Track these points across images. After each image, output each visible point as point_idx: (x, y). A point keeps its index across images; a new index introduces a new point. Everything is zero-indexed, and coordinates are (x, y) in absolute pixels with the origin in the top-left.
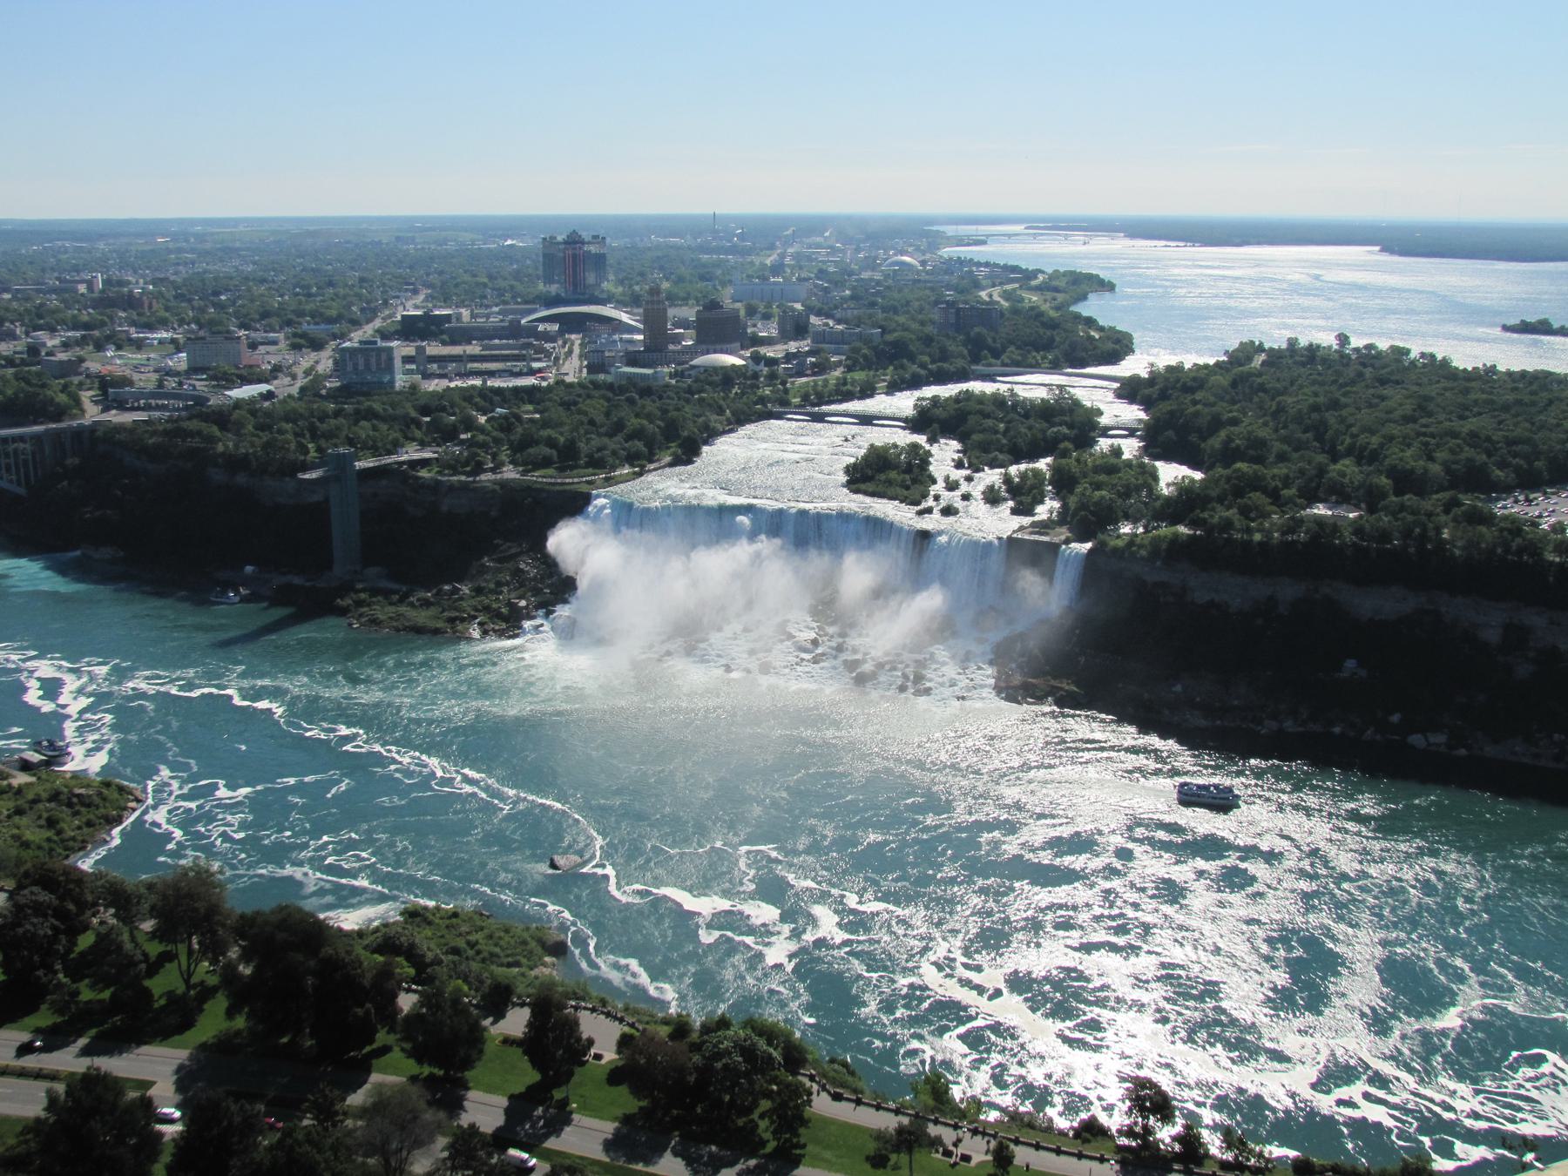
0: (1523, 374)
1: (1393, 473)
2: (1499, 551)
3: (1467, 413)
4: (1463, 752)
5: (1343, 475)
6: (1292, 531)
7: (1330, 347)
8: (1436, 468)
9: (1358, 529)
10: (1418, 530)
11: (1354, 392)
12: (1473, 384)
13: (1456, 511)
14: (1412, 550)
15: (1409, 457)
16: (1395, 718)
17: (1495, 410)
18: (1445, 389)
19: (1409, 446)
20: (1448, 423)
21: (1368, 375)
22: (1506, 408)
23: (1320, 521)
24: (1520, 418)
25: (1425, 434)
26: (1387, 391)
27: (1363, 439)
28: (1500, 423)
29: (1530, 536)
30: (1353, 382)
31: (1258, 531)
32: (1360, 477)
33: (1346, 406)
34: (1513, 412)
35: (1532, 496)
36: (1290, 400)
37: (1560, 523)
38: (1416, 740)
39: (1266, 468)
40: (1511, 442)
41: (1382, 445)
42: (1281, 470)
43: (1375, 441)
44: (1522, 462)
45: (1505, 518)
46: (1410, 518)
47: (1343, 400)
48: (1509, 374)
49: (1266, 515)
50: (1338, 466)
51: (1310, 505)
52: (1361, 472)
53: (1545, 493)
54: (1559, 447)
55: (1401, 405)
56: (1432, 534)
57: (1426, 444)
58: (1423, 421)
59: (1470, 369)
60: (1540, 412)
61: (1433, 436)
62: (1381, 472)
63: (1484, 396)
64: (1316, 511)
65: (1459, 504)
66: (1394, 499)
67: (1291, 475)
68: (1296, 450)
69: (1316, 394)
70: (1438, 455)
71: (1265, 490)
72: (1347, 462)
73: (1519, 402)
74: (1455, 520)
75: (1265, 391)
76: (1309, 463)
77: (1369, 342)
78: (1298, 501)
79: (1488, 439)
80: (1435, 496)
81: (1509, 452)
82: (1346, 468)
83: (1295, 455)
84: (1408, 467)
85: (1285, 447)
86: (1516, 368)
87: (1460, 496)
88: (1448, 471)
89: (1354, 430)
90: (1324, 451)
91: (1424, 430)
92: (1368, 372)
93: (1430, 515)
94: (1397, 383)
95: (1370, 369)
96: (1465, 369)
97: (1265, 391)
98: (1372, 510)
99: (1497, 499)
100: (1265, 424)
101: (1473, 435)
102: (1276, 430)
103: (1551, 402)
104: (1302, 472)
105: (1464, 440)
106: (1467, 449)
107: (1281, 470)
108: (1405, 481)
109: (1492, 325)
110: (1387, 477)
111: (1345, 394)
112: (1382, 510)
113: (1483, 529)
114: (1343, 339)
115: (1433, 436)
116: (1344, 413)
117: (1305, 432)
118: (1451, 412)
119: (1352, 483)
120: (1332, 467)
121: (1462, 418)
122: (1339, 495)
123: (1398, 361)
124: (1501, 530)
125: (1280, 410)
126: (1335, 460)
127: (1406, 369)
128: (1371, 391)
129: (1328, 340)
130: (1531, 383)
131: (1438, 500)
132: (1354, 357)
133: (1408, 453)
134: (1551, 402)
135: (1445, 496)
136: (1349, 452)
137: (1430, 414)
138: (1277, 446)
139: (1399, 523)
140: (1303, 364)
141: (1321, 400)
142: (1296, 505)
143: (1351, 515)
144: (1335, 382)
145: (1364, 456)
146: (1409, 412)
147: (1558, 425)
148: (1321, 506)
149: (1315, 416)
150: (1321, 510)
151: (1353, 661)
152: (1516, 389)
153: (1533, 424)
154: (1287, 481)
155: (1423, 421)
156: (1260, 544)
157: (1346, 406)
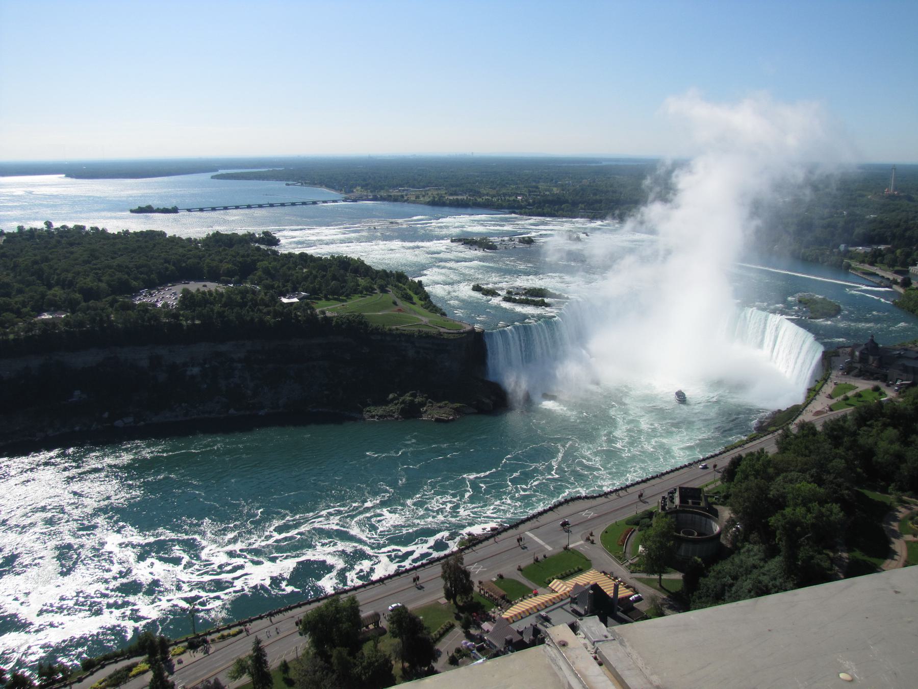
0: (142, 233)
1: (82, 291)
2: (140, 321)
3: (116, 255)
4: (142, 423)
5: (55, 296)
6: (30, 330)
7: (42, 229)
8: (103, 285)
9: (67, 322)
10: (98, 318)
11: (57, 252)
12: (117, 240)
13: (117, 305)
14: (97, 329)
15: (89, 282)
16: (106, 415)
17: (129, 252)
18: (104, 245)
19: (88, 276)
20: (106, 262)
21: (63, 242)
22: (134, 251)
23: (45, 322)
24: (141, 255)
25: (95, 269)
26: (75, 249)
27: (63, 276)
28: (132, 258)
29: (153, 312)
30: (56, 246)
31: (11, 333)
32: (64, 296)
33: (52, 259)
34: (137, 252)
35: (152, 292)
36: (21, 260)
37: (166, 303)
38: (119, 423)
39: (10, 298)
40: (138, 267)
41: (74, 277)
42: (20, 298)
43: (70, 276)
44: (145, 276)
45: (140, 305)
46: (93, 312)
47: (50, 256)
48: (135, 233)
49: (14, 324)
50: (52, 292)
51: (40, 314)
52: (65, 293)
53: (158, 290)
54: (161, 266)
55: (81, 255)
56: (105, 318)
57: (97, 274)
58: (94, 262)
59: (116, 233)
60: (150, 251)
61: (100, 269)
62: (75, 292)
63: (123, 246)
64: (43, 317)
65: (117, 301)
66: (83, 304)
67: (26, 300)
68: (28, 286)
69: (35, 255)
70: (103, 278)
71: (12, 311)
72: (56, 289)
73: (139, 247)
74: (116, 310)
75: (6, 256)
76: (36, 292)
77: (63, 224)
78: (32, 313)
79: (127, 267)
80: (104, 300)
81: (138, 272)
82: (57, 292)
83: (27, 289)
84: (89, 286)
85: (21, 286)
86: (138, 230)
87: (118, 297)
88: (109, 285)
89: (58, 271)
90: (44, 285)
91: (95, 266)
92: (64, 241)
93: (103, 309)
94: (79, 244)
95: (65, 239)
96: (114, 233)
97: (6, 256)
98: (73, 312)
99: (136, 296)
100: (8, 275)
101: (119, 266)
102: (15, 277)
103: (155, 246)
104: (32, 297)
105: (115, 269)
106: (117, 273)
107: (20, 298)
108: (89, 294)
109: (123, 210)
110: (79, 294)
111: (51, 253)
112: (78, 311)
113: (130, 312)
114: (49, 224)
115: (100, 269)
116: (51, 263)
117: (32, 275)
118: (108, 256)
119: (61, 299)
120: (49, 292)
121: (112, 258)
122: (53, 306)
123: (80, 233)
124: (139, 311)
125: (16, 266)
126: (50, 287)
127: (84, 236)
128: (65, 250)
129: (40, 225)
130: (146, 237)
131: (106, 301)
132: (55, 233)
133: (88, 279)
134: (155, 246)
135: (110, 298)
136: (58, 283)
137: (97, 258)
138: (16, 285)
139: (88, 316)
140: (28, 240)
141: (38, 258)
142: (31, 316)
143: (63, 316)
144: (45, 247)
145: (64, 284)
146: (87, 259)
147: (159, 256)
148: (46, 314)
149: (35, 267)
150: (46, 316)
151: (79, 391)
152: (138, 241)
153: (147, 257)
154: (24, 304)
155: (94, 262)
156: (14, 340)
157: (52, 259)
